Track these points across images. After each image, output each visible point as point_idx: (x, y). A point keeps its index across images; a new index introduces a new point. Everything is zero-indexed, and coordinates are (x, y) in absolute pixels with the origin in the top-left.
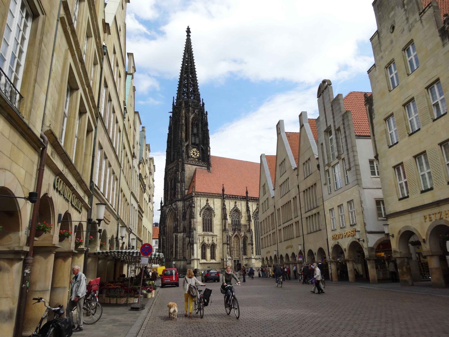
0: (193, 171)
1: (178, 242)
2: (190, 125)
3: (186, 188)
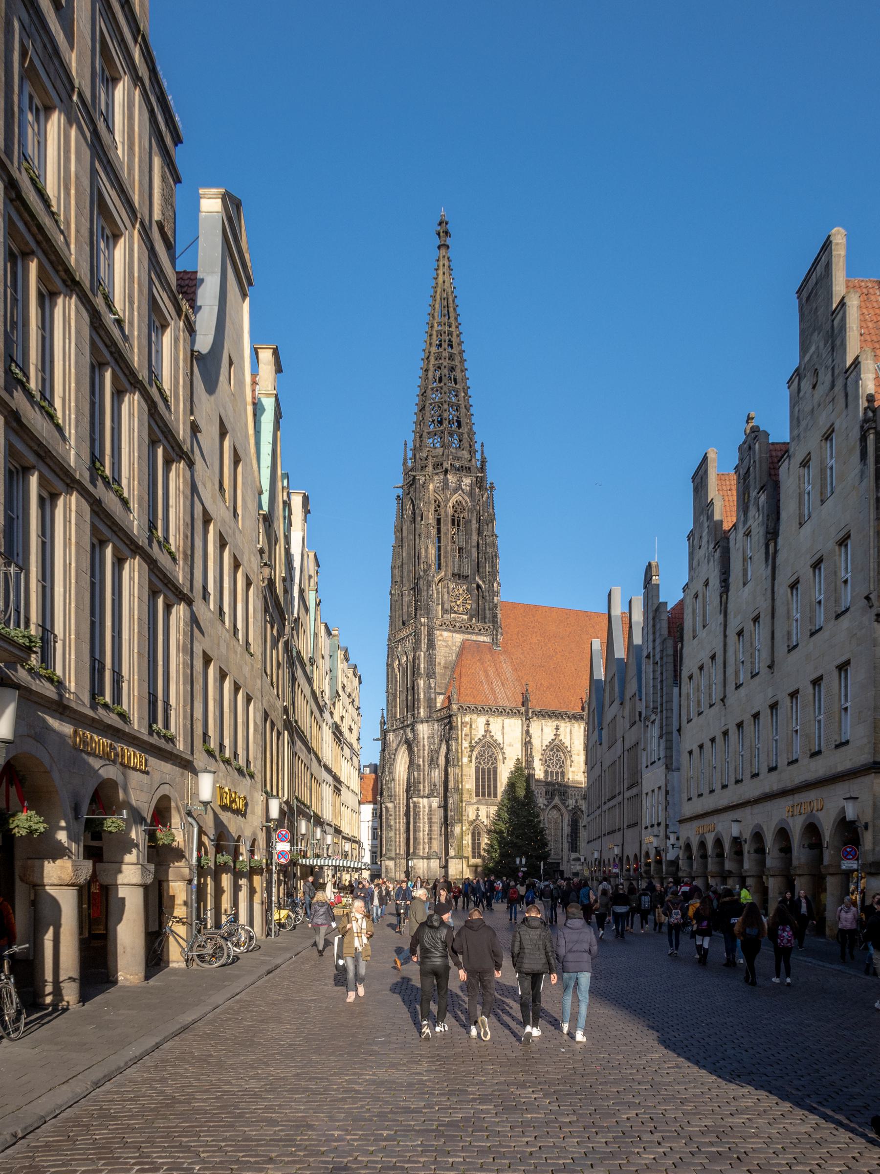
0: (455, 649)
1: (419, 819)
3: (438, 690)
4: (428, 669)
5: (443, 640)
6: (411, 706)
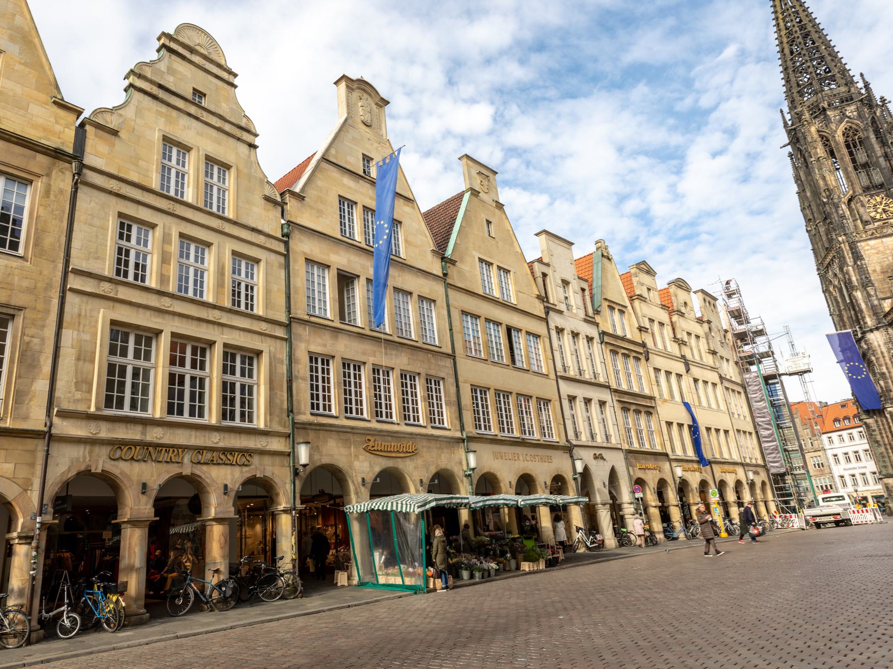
2: (845, 151)
3: (881, 296)
4: (861, 279)
5: (872, 248)
6: (858, 319)
